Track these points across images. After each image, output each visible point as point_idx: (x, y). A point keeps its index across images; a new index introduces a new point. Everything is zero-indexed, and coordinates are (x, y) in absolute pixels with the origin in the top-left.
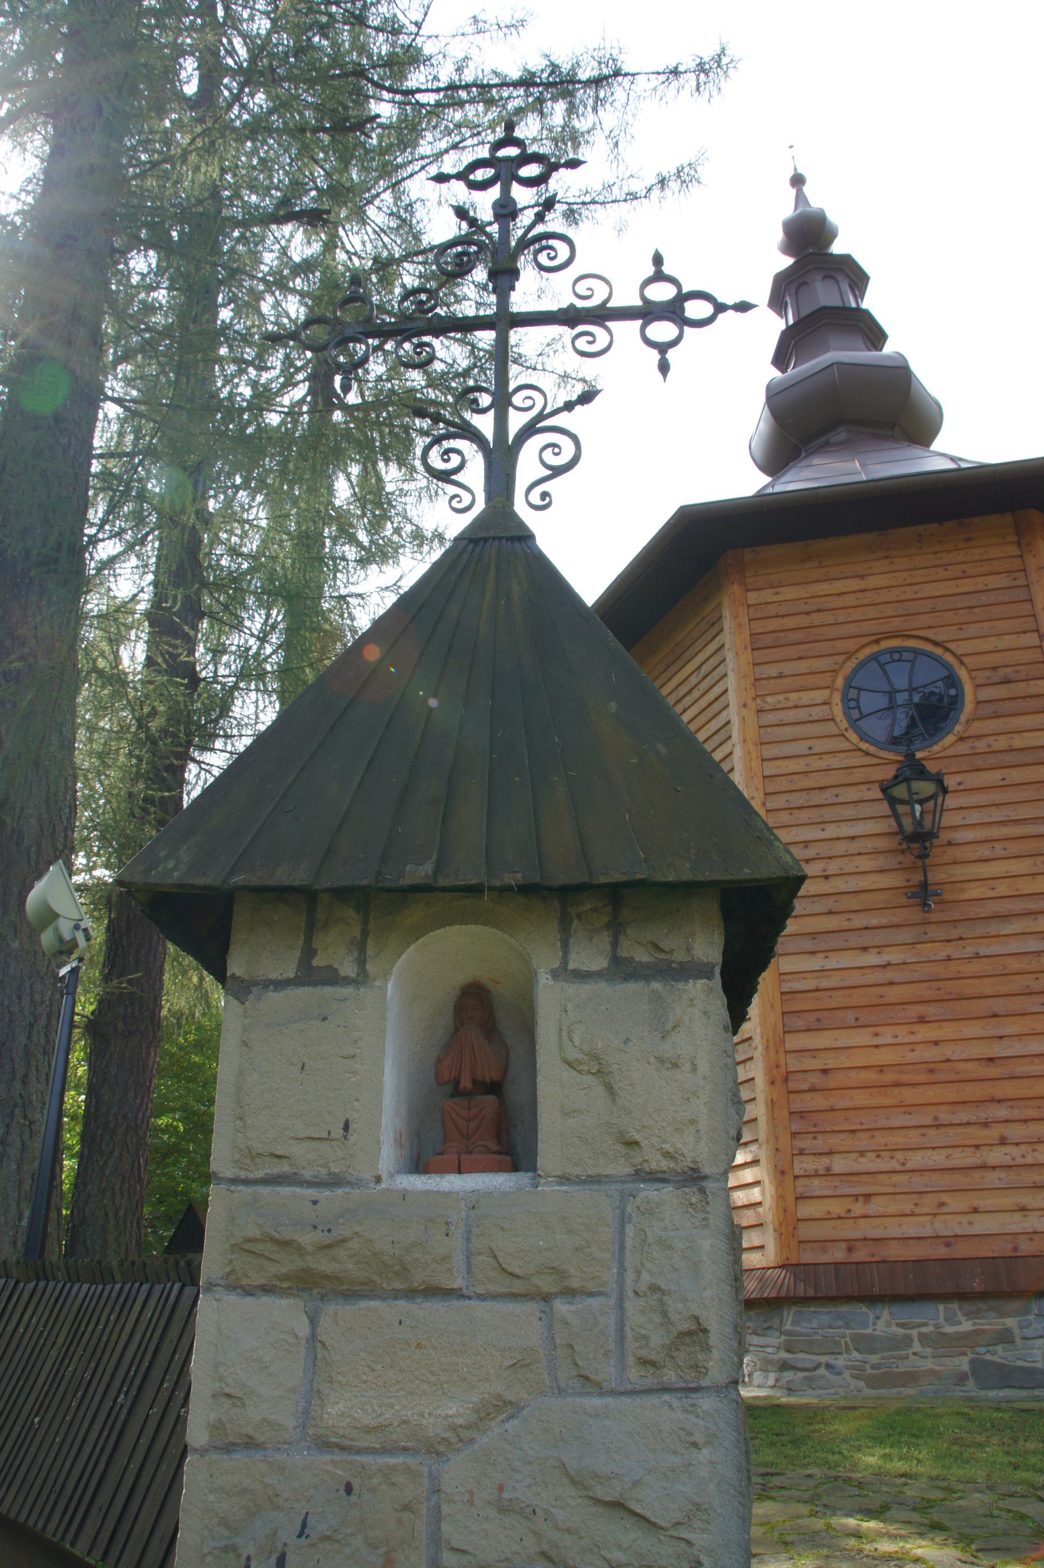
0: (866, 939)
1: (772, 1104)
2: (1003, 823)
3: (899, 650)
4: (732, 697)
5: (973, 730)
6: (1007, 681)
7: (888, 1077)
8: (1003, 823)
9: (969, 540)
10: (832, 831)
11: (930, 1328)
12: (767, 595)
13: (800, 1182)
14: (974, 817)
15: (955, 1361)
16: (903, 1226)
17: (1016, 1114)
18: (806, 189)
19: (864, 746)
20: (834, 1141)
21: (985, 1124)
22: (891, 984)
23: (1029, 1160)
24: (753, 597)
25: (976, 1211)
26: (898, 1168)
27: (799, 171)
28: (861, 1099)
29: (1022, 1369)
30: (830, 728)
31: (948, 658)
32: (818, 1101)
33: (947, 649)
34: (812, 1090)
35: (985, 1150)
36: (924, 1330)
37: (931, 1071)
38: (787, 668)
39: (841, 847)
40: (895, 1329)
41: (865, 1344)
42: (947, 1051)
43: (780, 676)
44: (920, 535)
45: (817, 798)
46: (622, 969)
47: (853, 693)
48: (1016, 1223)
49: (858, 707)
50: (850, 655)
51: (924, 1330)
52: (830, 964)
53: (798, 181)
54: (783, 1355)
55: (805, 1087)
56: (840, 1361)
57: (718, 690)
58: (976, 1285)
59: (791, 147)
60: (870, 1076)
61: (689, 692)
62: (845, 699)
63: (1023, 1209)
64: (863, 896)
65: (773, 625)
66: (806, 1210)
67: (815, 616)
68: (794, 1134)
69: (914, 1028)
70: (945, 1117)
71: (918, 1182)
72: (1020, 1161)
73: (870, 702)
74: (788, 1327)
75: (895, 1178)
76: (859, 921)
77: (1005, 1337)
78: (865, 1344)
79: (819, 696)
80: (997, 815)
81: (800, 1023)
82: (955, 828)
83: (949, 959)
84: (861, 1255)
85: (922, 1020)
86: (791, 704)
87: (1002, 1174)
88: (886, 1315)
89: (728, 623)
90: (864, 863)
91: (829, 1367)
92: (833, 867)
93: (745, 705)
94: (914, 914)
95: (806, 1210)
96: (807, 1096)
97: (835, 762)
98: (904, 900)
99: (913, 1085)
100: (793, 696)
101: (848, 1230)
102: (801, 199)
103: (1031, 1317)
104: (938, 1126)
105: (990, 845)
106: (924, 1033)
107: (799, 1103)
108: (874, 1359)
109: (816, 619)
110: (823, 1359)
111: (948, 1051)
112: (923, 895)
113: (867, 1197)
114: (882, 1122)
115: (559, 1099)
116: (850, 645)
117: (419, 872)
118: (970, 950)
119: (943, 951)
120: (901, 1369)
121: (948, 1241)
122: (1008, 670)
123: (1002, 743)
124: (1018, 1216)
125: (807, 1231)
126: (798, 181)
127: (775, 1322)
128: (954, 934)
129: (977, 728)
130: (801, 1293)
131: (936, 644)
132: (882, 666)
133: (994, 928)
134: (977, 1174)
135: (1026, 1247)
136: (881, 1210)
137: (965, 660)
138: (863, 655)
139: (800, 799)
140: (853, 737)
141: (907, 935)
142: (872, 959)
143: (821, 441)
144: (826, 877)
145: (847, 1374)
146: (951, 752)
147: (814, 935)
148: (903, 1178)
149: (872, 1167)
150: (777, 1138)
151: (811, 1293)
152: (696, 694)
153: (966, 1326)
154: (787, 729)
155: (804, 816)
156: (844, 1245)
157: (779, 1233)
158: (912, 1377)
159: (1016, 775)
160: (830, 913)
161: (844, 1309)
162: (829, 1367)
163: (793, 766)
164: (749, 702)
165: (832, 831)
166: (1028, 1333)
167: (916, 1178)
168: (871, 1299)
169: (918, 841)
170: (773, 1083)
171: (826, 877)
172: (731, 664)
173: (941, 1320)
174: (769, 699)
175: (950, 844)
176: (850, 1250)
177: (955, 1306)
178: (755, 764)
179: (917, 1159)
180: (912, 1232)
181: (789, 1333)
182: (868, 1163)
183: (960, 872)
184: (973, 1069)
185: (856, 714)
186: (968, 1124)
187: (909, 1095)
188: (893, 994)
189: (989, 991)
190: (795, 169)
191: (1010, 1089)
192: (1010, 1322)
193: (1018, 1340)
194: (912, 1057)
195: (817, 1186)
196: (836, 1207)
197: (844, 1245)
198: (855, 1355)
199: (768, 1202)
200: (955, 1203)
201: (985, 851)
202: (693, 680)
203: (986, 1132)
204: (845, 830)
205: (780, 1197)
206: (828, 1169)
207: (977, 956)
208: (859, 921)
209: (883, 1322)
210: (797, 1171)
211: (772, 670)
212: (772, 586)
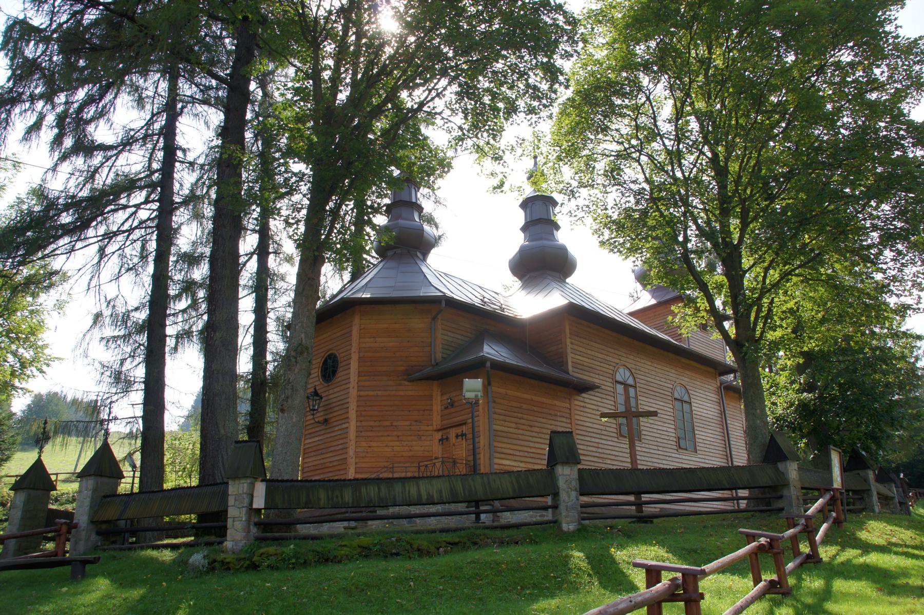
106: (322, 456)
111: (325, 461)
141: (323, 432)
188: (319, 447)
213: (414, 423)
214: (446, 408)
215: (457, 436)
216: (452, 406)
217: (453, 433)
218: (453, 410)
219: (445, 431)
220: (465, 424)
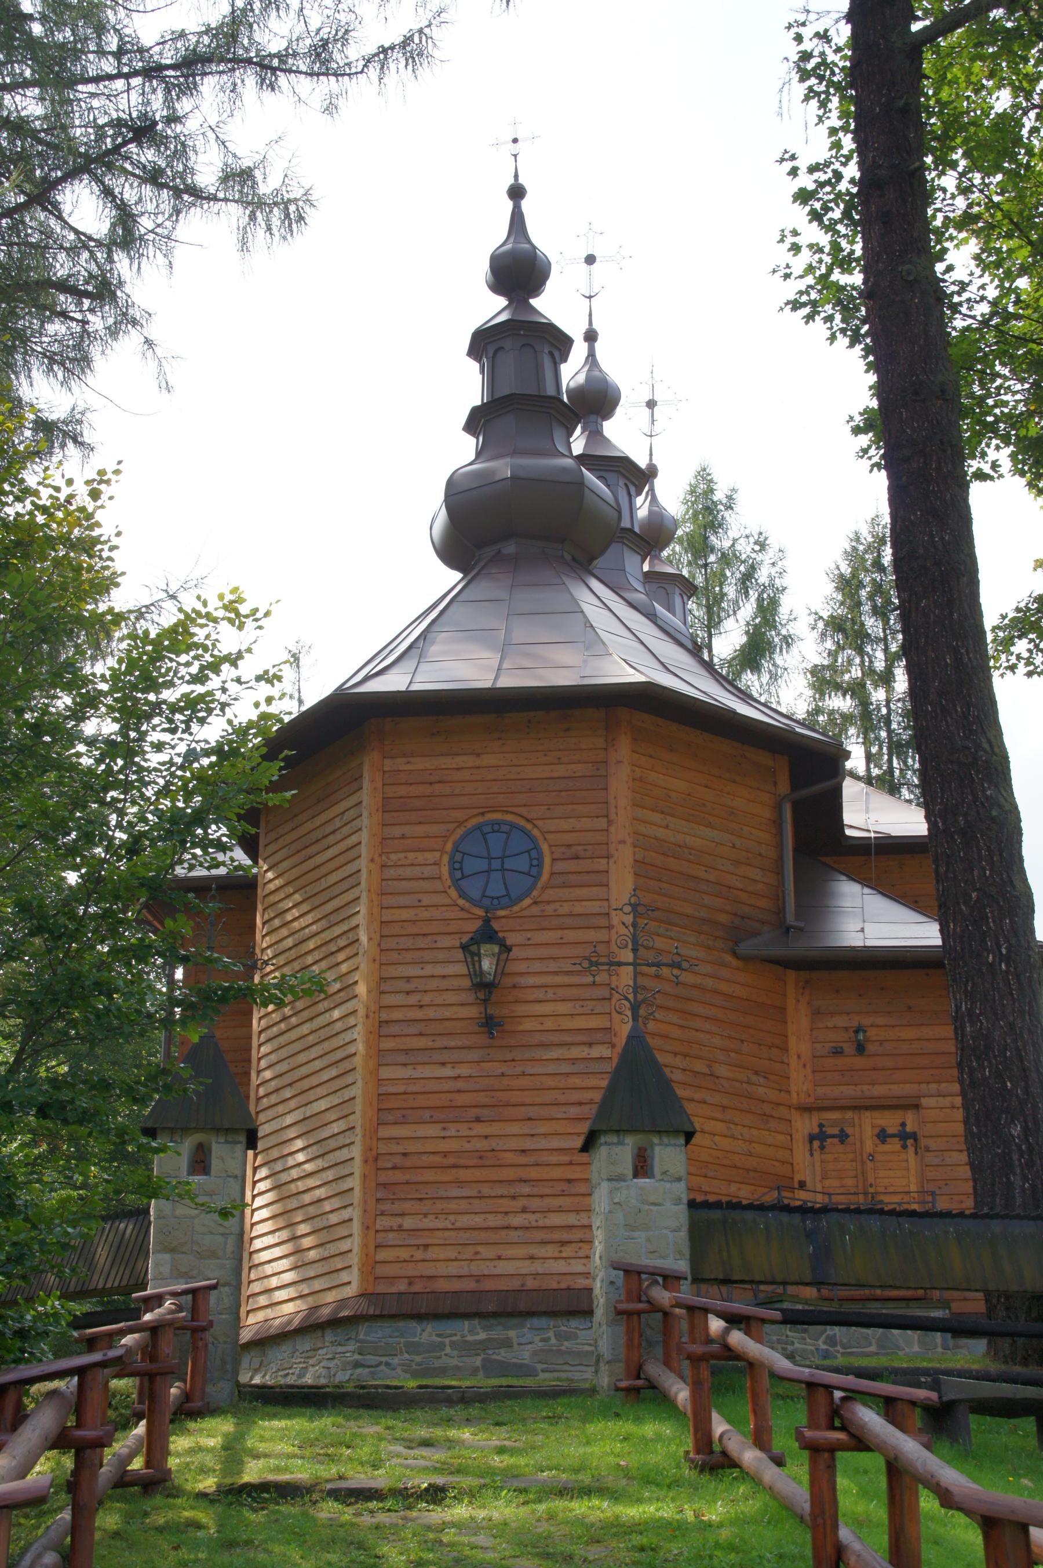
0: (445, 1056)
1: (365, 1177)
2: (556, 973)
3: (498, 823)
4: (363, 849)
5: (545, 897)
6: (577, 857)
7: (450, 1160)
8: (556, 973)
9: (567, 730)
10: (429, 970)
11: (458, 1338)
12: (400, 763)
13: (380, 1235)
14: (537, 967)
15: (472, 1359)
16: (449, 1268)
17: (535, 1191)
18: (525, 204)
19: (461, 902)
20: (407, 1206)
21: (514, 1197)
22: (459, 1091)
23: (541, 1223)
24: (388, 765)
25: (499, 1258)
26: (450, 1226)
27: (521, 181)
28: (429, 1176)
29: (515, 1364)
30: (438, 886)
31: (535, 832)
32: (399, 1176)
33: (535, 826)
34: (394, 1168)
35: (511, 1216)
36: (454, 1338)
37: (481, 1158)
38: (408, 830)
39: (434, 984)
40: (435, 1338)
41: (413, 1348)
42: (494, 1143)
43: (403, 837)
44: (529, 722)
45: (421, 943)
46: (227, 1142)
47: (458, 857)
48: (526, 1267)
49: (461, 869)
50: (460, 824)
51: (454, 1338)
52: (416, 1074)
53: (517, 193)
54: (357, 1357)
55: (389, 1165)
56: (395, 1361)
57: (354, 839)
58: (490, 1308)
59: (515, 141)
60: (437, 1159)
61: (334, 832)
62: (452, 862)
63: (532, 1258)
64: (447, 1024)
65: (402, 791)
67: (437, 786)
68: (378, 1200)
69: (471, 1125)
70: (486, 1190)
71: (463, 1237)
72: (534, 1224)
73: (473, 865)
74: (361, 1337)
75: (447, 1234)
76: (440, 1042)
77: (507, 1344)
78: (413, 1348)
79: (432, 857)
80: (553, 966)
81: (390, 1118)
82: (521, 974)
83: (503, 1075)
84: (417, 1287)
85: (478, 1120)
86: (408, 862)
87: (519, 1233)
88: (429, 1329)
89: (366, 784)
90: (451, 998)
91: (387, 1364)
92: (426, 999)
93: (372, 860)
95: (382, 1255)
96: (390, 1172)
97: (437, 914)
98: (476, 1028)
99: (466, 1167)
100: (411, 855)
101: (410, 1270)
102: (517, 222)
103: (526, 1330)
104: (480, 1198)
105: (543, 990)
107: (383, 1178)
108: (418, 1358)
109: (438, 788)
110: (384, 1359)
111: (494, 1143)
112: (490, 1024)
113: (426, 1246)
114: (442, 1193)
115: (215, 1164)
116: (459, 815)
117: (193, 1125)
118: (519, 1070)
119: (499, 1068)
120: (436, 1365)
121: (479, 1278)
122: (580, 848)
123: (565, 909)
124: (527, 1262)
125: (381, 1270)
126: (517, 193)
127: (353, 1335)
128: (509, 1057)
129: (551, 894)
130: (371, 1312)
131: (528, 820)
132: (484, 835)
133: (539, 1054)
134: (503, 1233)
135: (530, 1284)
136: (435, 1256)
137: (548, 836)
138: (470, 824)
140: (453, 893)
141: (474, 1055)
142: (447, 1072)
143: (489, 551)
144: (421, 1006)
145: (399, 1370)
146: (526, 913)
147: (406, 1051)
148: (452, 1233)
149: (432, 1225)
150: (365, 1202)
151: (378, 1312)
152: (338, 836)
153: (482, 1336)
154: (404, 883)
155: (409, 956)
156: (406, 1280)
157: (362, 1272)
158: (443, 1371)
159: (571, 936)
160: (421, 1034)
161: (401, 1324)
162: (387, 1364)
163: (405, 914)
164: (376, 858)
165: (429, 970)
166: (523, 1341)
167: (462, 1234)
168: (419, 1317)
169: (485, 988)
170: (366, 1161)
171: (421, 1006)
172: (365, 821)
173: (466, 1332)
174: (393, 857)
175: (514, 987)
176: (410, 1284)
177: (476, 1322)
178: (376, 910)
179: (463, 1221)
180: (455, 1272)
181: (361, 1341)
182: (429, 1223)
183: (521, 1009)
184: (510, 1158)
186: (502, 1196)
187: (464, 1174)
188: (461, 1099)
189: (528, 1101)
190: (516, 176)
191: (534, 1173)
192: (512, 1334)
193: (515, 1346)
194: (468, 1146)
195: (392, 1238)
196: (404, 1254)
197: (406, 1280)
198: (406, 1356)
199: (356, 1249)
200: (486, 1252)
201: (540, 994)
202: (338, 823)
203: (513, 1203)
204: (440, 970)
205: (364, 1246)
206: (400, 1226)
207: (524, 1074)
208: (440, 1042)
209: (427, 1333)
210: (378, 1227)
211: (397, 831)
212: (404, 756)
213: (754, 1078)
214: (838, 1052)
215: (883, 1136)
216: (860, 1049)
217: (867, 1125)
218: (859, 1062)
220: (917, 1107)
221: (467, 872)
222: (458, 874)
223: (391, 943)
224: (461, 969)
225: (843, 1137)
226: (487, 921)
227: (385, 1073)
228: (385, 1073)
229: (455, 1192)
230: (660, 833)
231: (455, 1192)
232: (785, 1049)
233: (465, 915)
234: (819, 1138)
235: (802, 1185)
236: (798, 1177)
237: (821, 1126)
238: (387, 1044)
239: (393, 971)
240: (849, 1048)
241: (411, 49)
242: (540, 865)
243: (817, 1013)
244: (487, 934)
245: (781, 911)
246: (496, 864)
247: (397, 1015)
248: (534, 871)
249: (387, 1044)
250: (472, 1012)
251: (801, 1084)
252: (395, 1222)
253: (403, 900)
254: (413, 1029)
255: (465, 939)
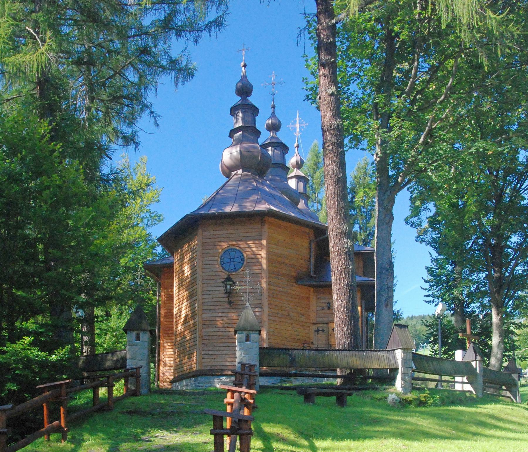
7: (220, 337)
12: (207, 233)
19: (223, 270)
24: (204, 233)
32: (208, 341)
45: (213, 281)
65: (207, 240)
66: (204, 360)
84: (212, 368)
90: (220, 296)
92: (214, 296)
94: (228, 306)
95: (204, 360)
107: (204, 341)
125: (204, 364)
139: (209, 281)
140: (221, 268)
163: (209, 274)
169: (229, 293)
174: (206, 258)
182: (216, 353)
185: (222, 263)
187: (224, 341)
194: (225, 334)
196: (209, 360)
204: (218, 288)
211: (207, 251)
214: (323, 309)
219: (321, 325)
221: (225, 262)
222: (222, 263)
223: (205, 281)
224: (222, 288)
225: (323, 331)
226: (229, 275)
227: (204, 315)
228: (204, 315)
229: (222, 345)
230: (276, 251)
231: (222, 345)
232: (309, 308)
233: (223, 274)
234: (318, 331)
235: (312, 342)
236: (311, 341)
237: (318, 328)
238: (205, 308)
239: (205, 289)
240: (326, 308)
241: (218, 23)
242: (244, 261)
243: (318, 299)
244: (229, 279)
245: (310, 272)
246: (232, 260)
247: (206, 300)
248: (242, 262)
249: (205, 308)
250: (227, 299)
251: (313, 317)
252: (207, 353)
253: (208, 270)
254: (211, 304)
255: (223, 280)
